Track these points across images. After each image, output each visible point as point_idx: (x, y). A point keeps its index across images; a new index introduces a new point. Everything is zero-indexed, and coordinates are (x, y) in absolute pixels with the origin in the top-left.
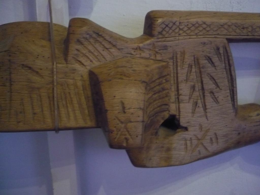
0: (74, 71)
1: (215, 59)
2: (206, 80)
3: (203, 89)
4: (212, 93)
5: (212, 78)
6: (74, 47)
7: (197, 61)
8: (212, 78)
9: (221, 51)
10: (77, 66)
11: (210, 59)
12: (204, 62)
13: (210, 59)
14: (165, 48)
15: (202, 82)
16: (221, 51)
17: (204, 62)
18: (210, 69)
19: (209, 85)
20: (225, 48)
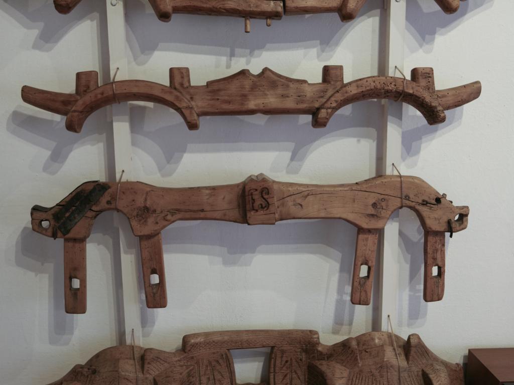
0: (147, 378)
1: (221, 361)
2: (216, 373)
3: (214, 379)
4: (220, 381)
5: (220, 372)
6: (146, 366)
7: (210, 363)
8: (220, 372)
9: (224, 356)
10: (148, 376)
11: (218, 362)
12: (214, 363)
13: (218, 362)
14: (192, 358)
15: (214, 375)
16: (224, 356)
17: (214, 363)
18: (218, 367)
19: (218, 377)
20: (226, 354)
